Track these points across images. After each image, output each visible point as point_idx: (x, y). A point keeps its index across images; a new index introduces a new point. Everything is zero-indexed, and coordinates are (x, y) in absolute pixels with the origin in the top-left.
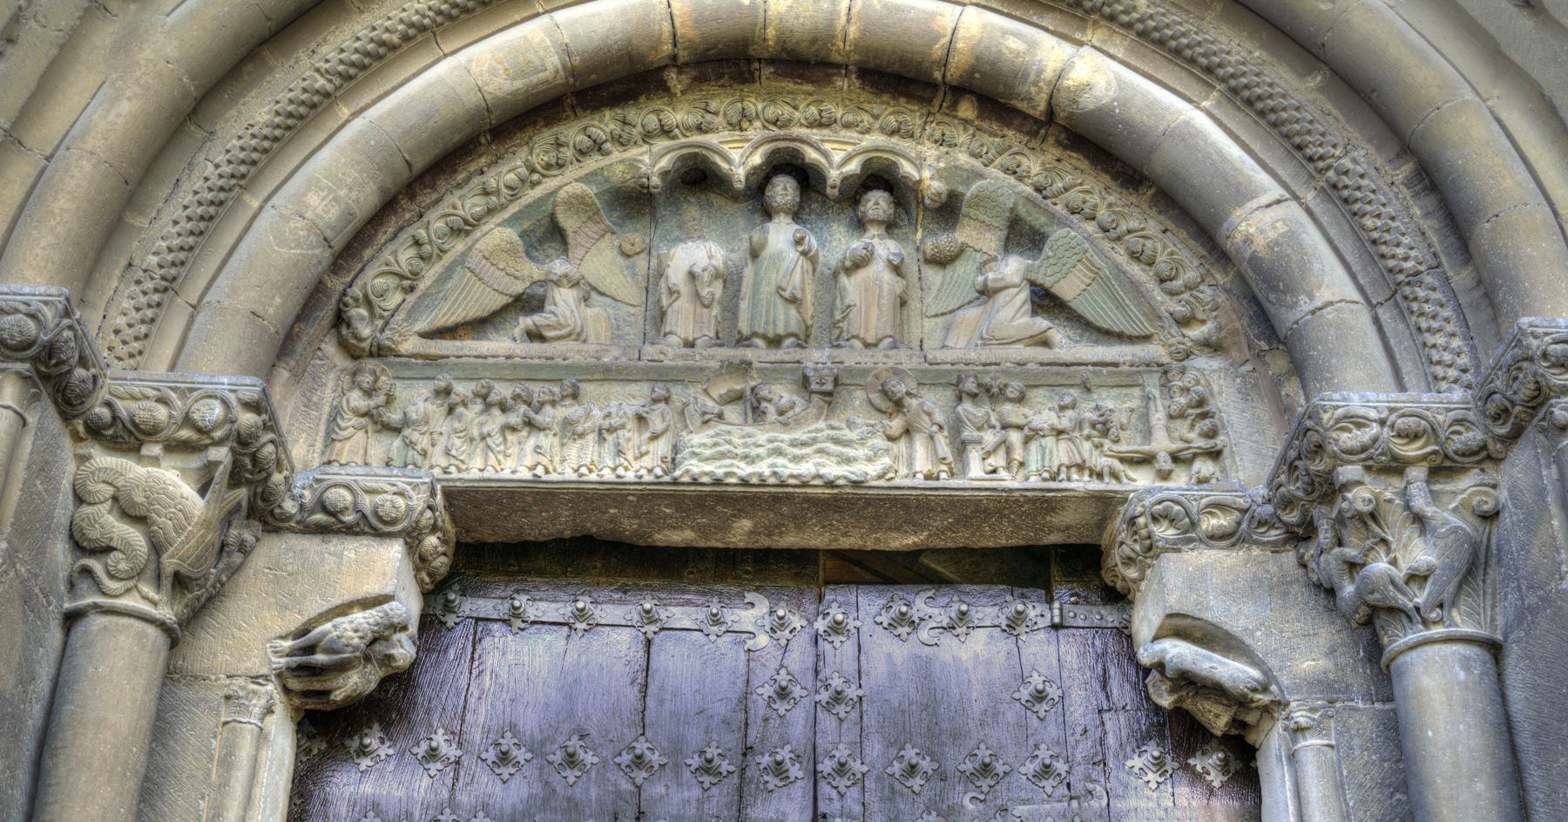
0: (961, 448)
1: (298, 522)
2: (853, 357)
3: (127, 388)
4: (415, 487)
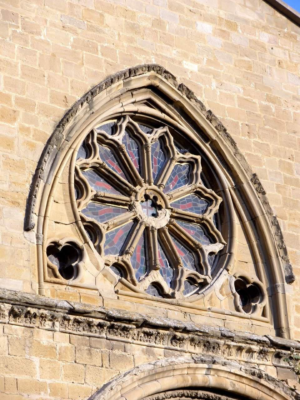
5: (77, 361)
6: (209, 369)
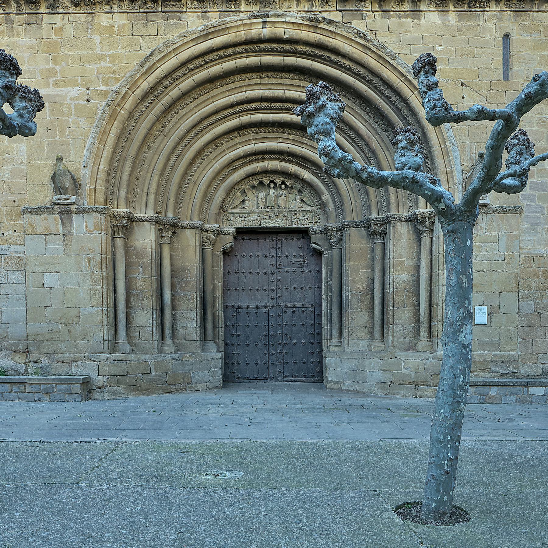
0: (292, 222)
2: (280, 210)
3: (207, 227)
5: (134, 34)
6: (265, 23)
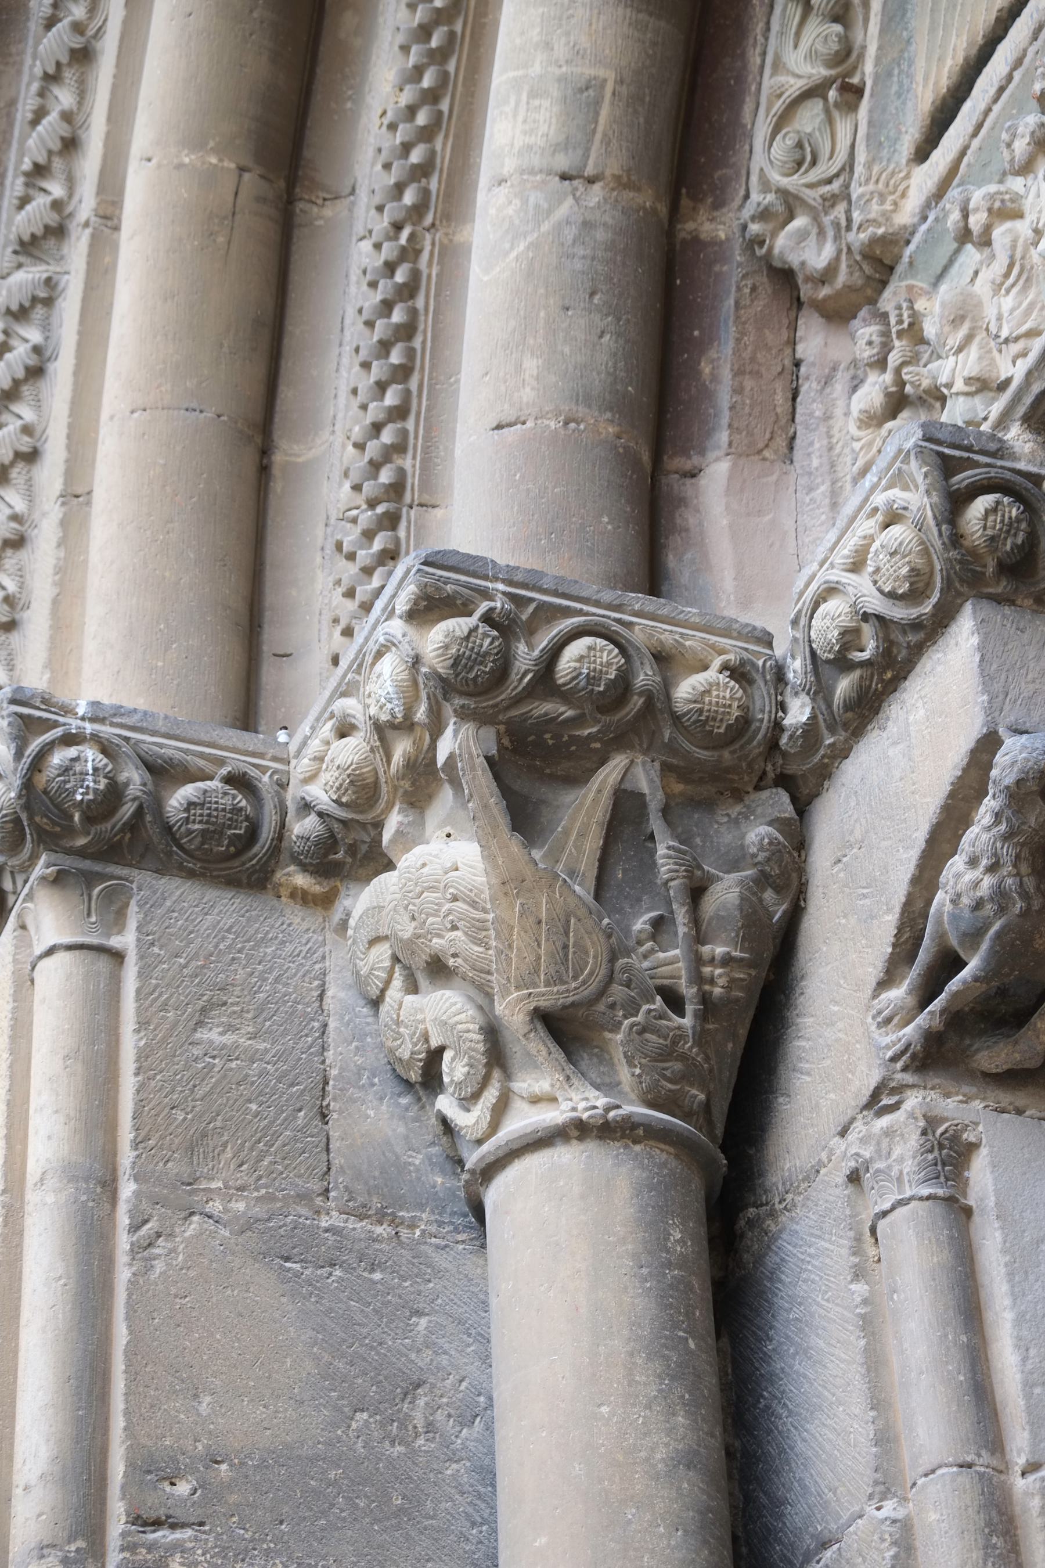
1: (832, 729)
4: (900, 480)
